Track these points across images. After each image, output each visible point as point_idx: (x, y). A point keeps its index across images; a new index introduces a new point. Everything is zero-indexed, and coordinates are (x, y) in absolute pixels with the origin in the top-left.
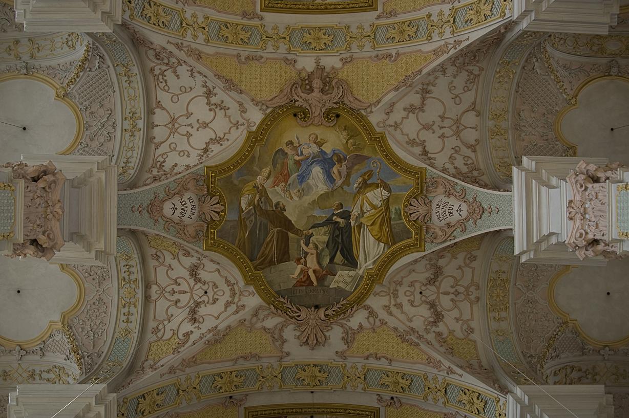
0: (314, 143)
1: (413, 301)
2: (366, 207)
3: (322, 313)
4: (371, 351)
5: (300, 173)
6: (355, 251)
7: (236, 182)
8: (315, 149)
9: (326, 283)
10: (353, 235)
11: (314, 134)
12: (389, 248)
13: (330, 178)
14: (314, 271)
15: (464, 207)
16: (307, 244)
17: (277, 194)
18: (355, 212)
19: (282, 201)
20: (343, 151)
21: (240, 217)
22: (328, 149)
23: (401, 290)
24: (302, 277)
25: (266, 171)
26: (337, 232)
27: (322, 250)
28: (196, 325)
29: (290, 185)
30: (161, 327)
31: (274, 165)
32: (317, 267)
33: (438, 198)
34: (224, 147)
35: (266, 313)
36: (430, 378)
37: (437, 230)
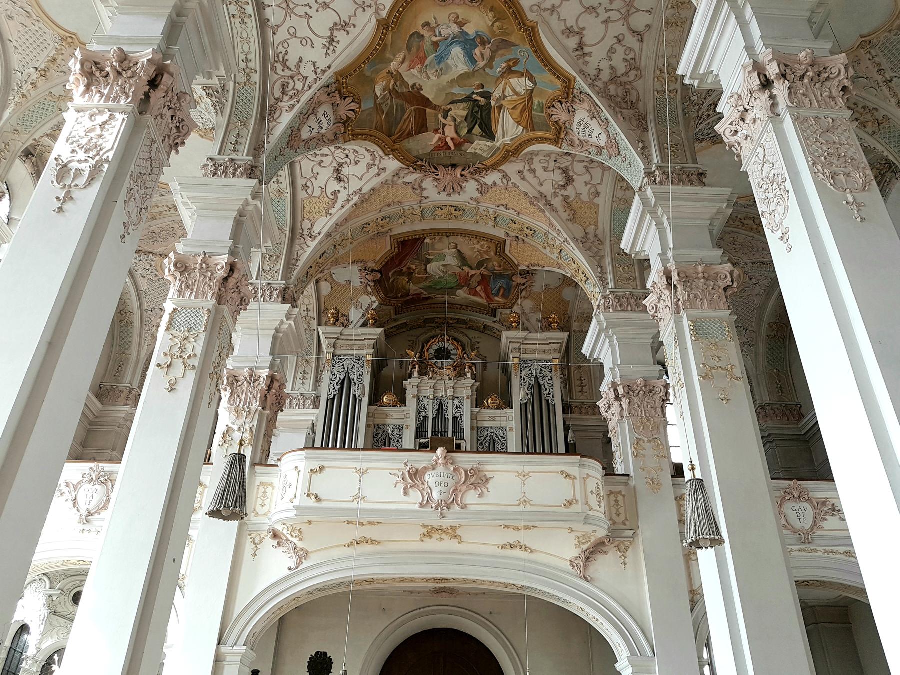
0: (456, 23)
1: (547, 168)
2: (509, 92)
3: (458, 172)
4: (503, 202)
5: (439, 54)
6: (494, 128)
7: (368, 74)
8: (456, 29)
9: (463, 149)
10: (493, 113)
11: (455, 13)
12: (528, 132)
13: (473, 61)
14: (452, 139)
15: (604, 138)
16: (445, 118)
17: (412, 77)
18: (497, 94)
19: (419, 82)
20: (488, 34)
21: (376, 102)
22: (470, 30)
23: (536, 160)
24: (440, 143)
25: (400, 57)
26: (477, 109)
27: (461, 123)
28: (342, 184)
29: (426, 67)
30: (309, 184)
31: (409, 49)
32: (455, 136)
33: (582, 114)
34: (352, 37)
35: (406, 172)
36: (550, 237)
37: (576, 139)
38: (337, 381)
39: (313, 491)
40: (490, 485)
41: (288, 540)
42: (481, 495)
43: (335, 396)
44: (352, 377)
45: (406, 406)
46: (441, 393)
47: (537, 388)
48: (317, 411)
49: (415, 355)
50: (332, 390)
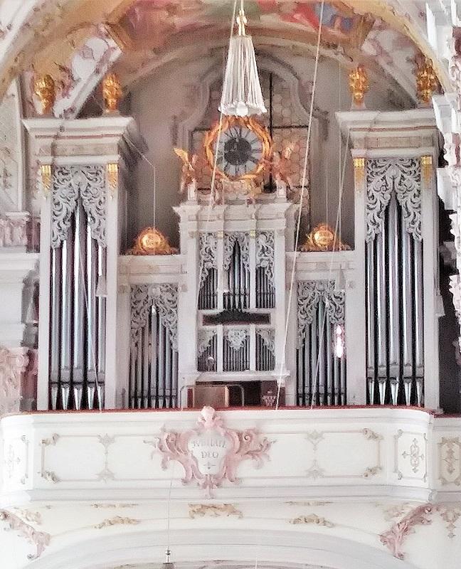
38: (64, 213)
39: (47, 469)
40: (273, 451)
41: (22, 523)
42: (259, 467)
43: (62, 242)
44: (88, 208)
45: (179, 252)
46: (234, 228)
47: (393, 212)
48: (34, 256)
49: (190, 159)
50: (56, 233)
